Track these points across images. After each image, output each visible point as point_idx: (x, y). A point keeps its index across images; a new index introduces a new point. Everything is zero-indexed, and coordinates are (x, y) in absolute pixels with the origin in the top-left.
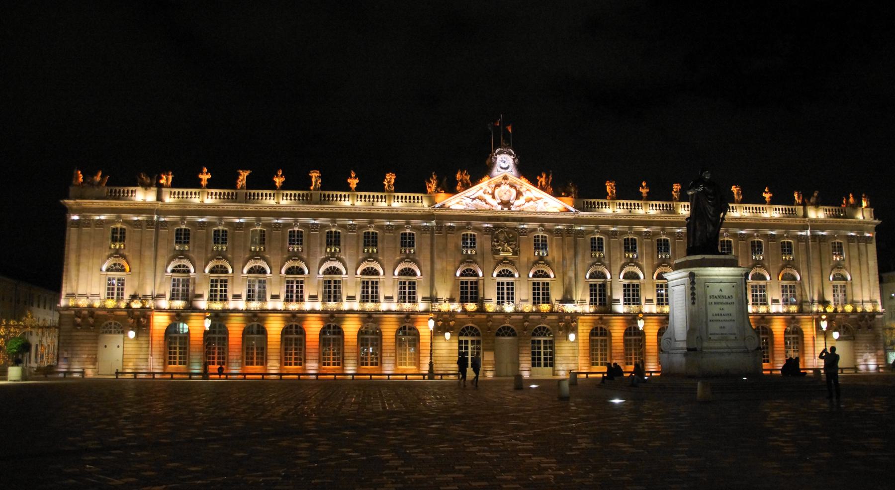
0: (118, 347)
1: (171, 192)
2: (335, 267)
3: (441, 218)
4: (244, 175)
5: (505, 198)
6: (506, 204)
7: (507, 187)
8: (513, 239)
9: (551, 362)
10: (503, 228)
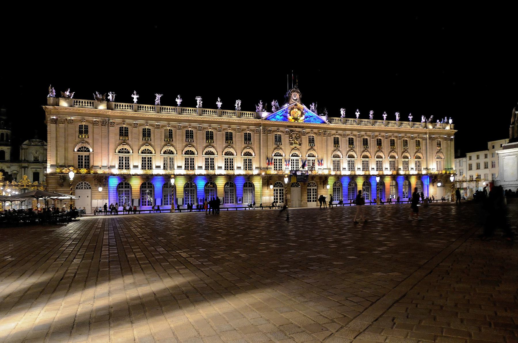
0: (88, 197)
2: (210, 151)
3: (265, 125)
5: (296, 116)
6: (296, 119)
7: (297, 110)
10: (294, 131)
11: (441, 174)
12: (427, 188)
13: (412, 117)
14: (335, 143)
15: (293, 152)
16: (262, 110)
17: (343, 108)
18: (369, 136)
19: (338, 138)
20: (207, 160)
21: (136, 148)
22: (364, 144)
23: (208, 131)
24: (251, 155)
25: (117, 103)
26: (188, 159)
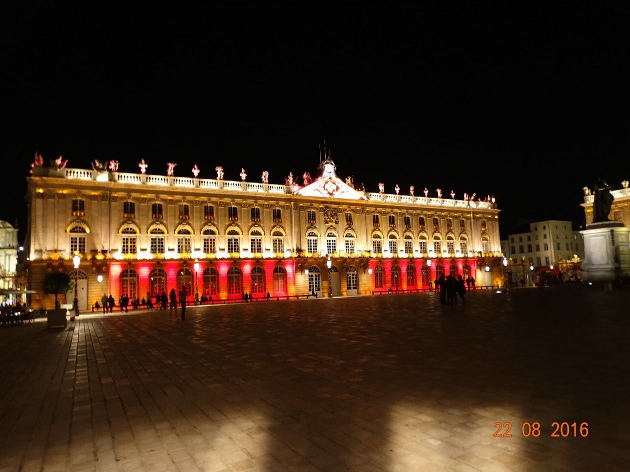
0: (83, 289)
2: (234, 231)
3: (297, 201)
5: (331, 191)
9: (357, 286)
11: (488, 257)
13: (454, 194)
14: (374, 222)
15: (329, 231)
16: (293, 183)
17: (382, 182)
18: (411, 214)
19: (377, 216)
20: (230, 241)
21: (144, 228)
22: (405, 224)
24: (282, 235)
25: (121, 174)
26: (208, 240)
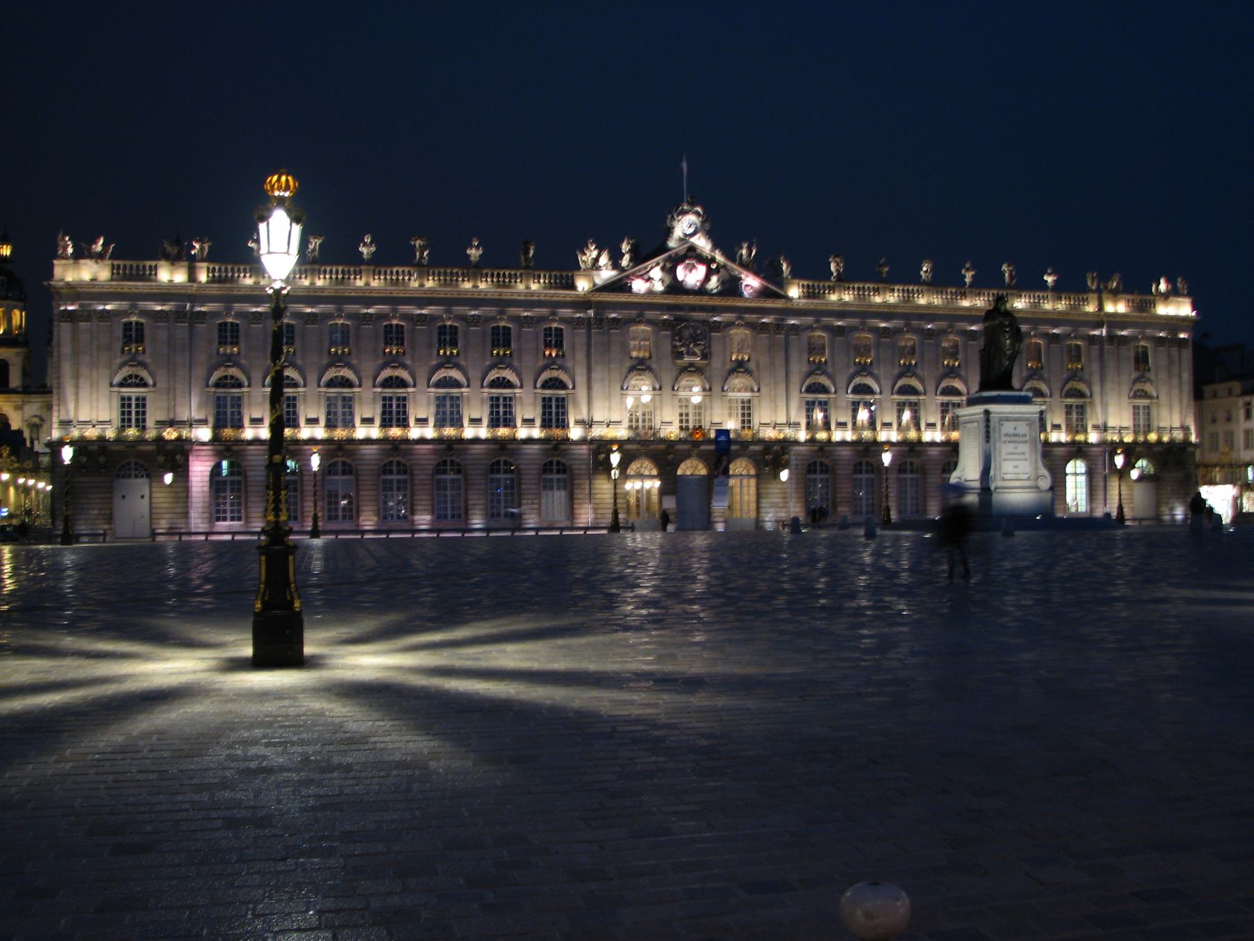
0: (142, 497)
1: (208, 269)
4: (316, 243)
8: (700, 337)
12: (1102, 484)
23: (551, 328)
24: (564, 387)
